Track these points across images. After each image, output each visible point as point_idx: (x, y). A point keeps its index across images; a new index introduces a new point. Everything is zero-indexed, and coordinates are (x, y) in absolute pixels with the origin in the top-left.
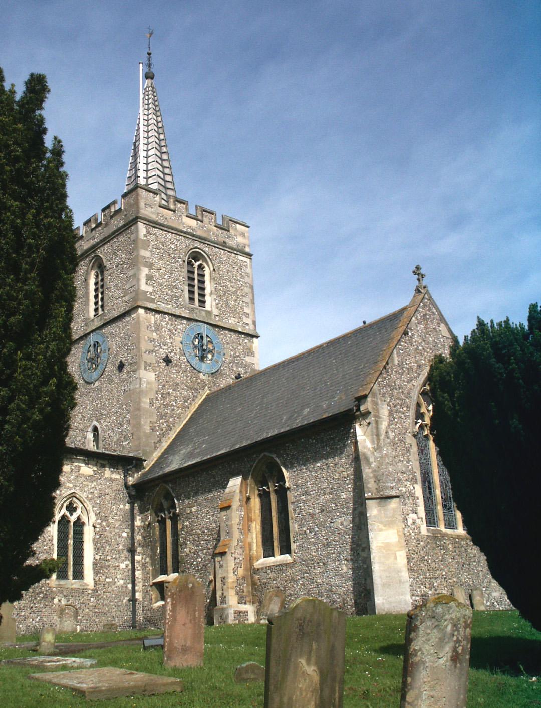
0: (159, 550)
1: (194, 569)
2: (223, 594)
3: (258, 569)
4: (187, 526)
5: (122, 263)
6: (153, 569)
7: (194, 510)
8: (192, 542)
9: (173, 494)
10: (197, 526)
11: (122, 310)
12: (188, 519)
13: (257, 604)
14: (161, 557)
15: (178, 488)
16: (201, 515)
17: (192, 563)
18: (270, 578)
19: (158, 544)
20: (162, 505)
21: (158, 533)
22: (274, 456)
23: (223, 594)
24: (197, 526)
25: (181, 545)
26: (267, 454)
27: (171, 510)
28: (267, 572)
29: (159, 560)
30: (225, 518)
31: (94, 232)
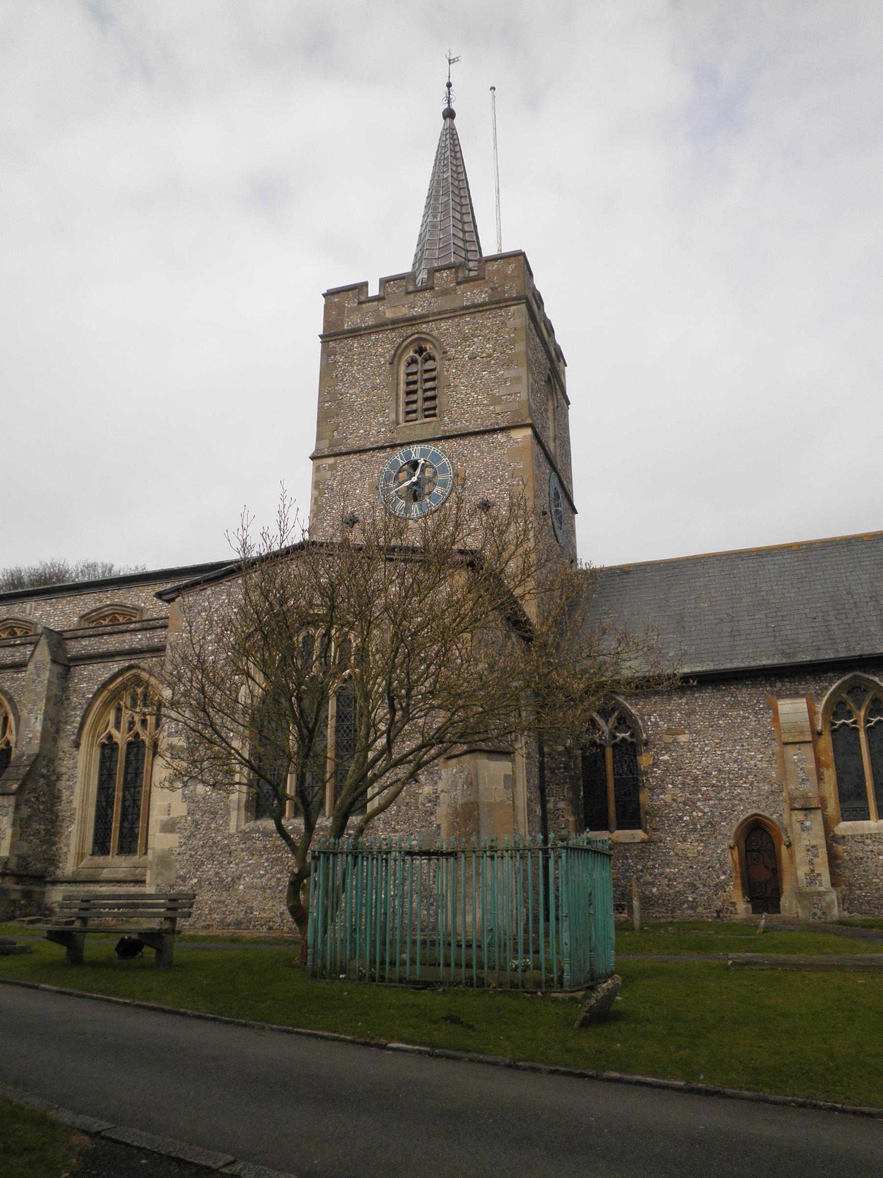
0: (582, 793)
1: (683, 827)
2: (813, 871)
3: (844, 837)
4: (666, 762)
5: (484, 355)
6: (576, 821)
7: (682, 738)
8: (680, 786)
9: (633, 711)
10: (690, 763)
11: (488, 424)
12: (667, 749)
13: (843, 887)
14: (585, 803)
15: (641, 703)
16: (702, 749)
17: (681, 818)
18: (872, 851)
19: (581, 782)
20: (593, 722)
21: (580, 765)
22: (876, 679)
23: (813, 871)
24: (690, 763)
25: (652, 789)
26: (858, 673)
27: (618, 734)
28: (864, 842)
29: (582, 806)
30: (795, 757)
31: (412, 296)
